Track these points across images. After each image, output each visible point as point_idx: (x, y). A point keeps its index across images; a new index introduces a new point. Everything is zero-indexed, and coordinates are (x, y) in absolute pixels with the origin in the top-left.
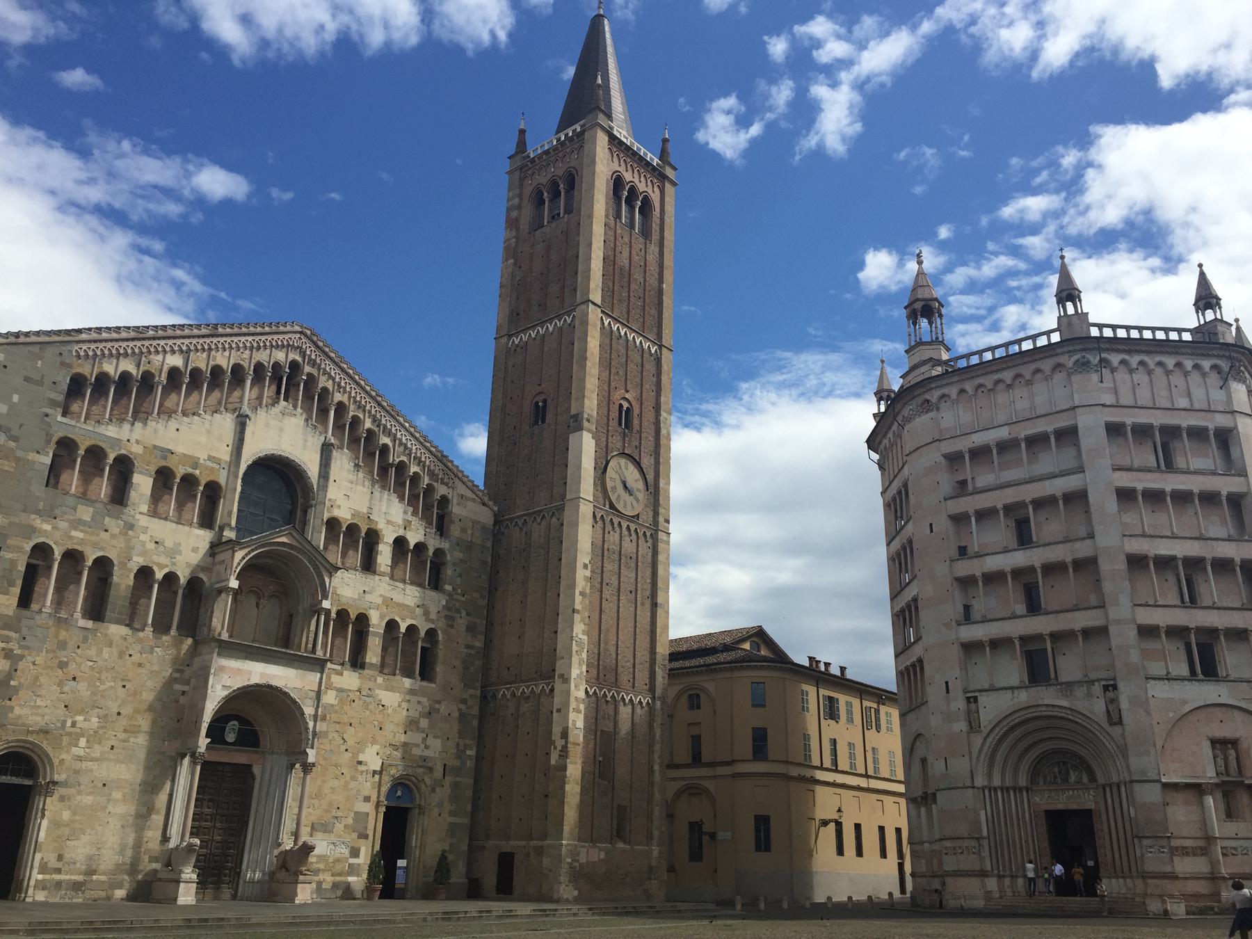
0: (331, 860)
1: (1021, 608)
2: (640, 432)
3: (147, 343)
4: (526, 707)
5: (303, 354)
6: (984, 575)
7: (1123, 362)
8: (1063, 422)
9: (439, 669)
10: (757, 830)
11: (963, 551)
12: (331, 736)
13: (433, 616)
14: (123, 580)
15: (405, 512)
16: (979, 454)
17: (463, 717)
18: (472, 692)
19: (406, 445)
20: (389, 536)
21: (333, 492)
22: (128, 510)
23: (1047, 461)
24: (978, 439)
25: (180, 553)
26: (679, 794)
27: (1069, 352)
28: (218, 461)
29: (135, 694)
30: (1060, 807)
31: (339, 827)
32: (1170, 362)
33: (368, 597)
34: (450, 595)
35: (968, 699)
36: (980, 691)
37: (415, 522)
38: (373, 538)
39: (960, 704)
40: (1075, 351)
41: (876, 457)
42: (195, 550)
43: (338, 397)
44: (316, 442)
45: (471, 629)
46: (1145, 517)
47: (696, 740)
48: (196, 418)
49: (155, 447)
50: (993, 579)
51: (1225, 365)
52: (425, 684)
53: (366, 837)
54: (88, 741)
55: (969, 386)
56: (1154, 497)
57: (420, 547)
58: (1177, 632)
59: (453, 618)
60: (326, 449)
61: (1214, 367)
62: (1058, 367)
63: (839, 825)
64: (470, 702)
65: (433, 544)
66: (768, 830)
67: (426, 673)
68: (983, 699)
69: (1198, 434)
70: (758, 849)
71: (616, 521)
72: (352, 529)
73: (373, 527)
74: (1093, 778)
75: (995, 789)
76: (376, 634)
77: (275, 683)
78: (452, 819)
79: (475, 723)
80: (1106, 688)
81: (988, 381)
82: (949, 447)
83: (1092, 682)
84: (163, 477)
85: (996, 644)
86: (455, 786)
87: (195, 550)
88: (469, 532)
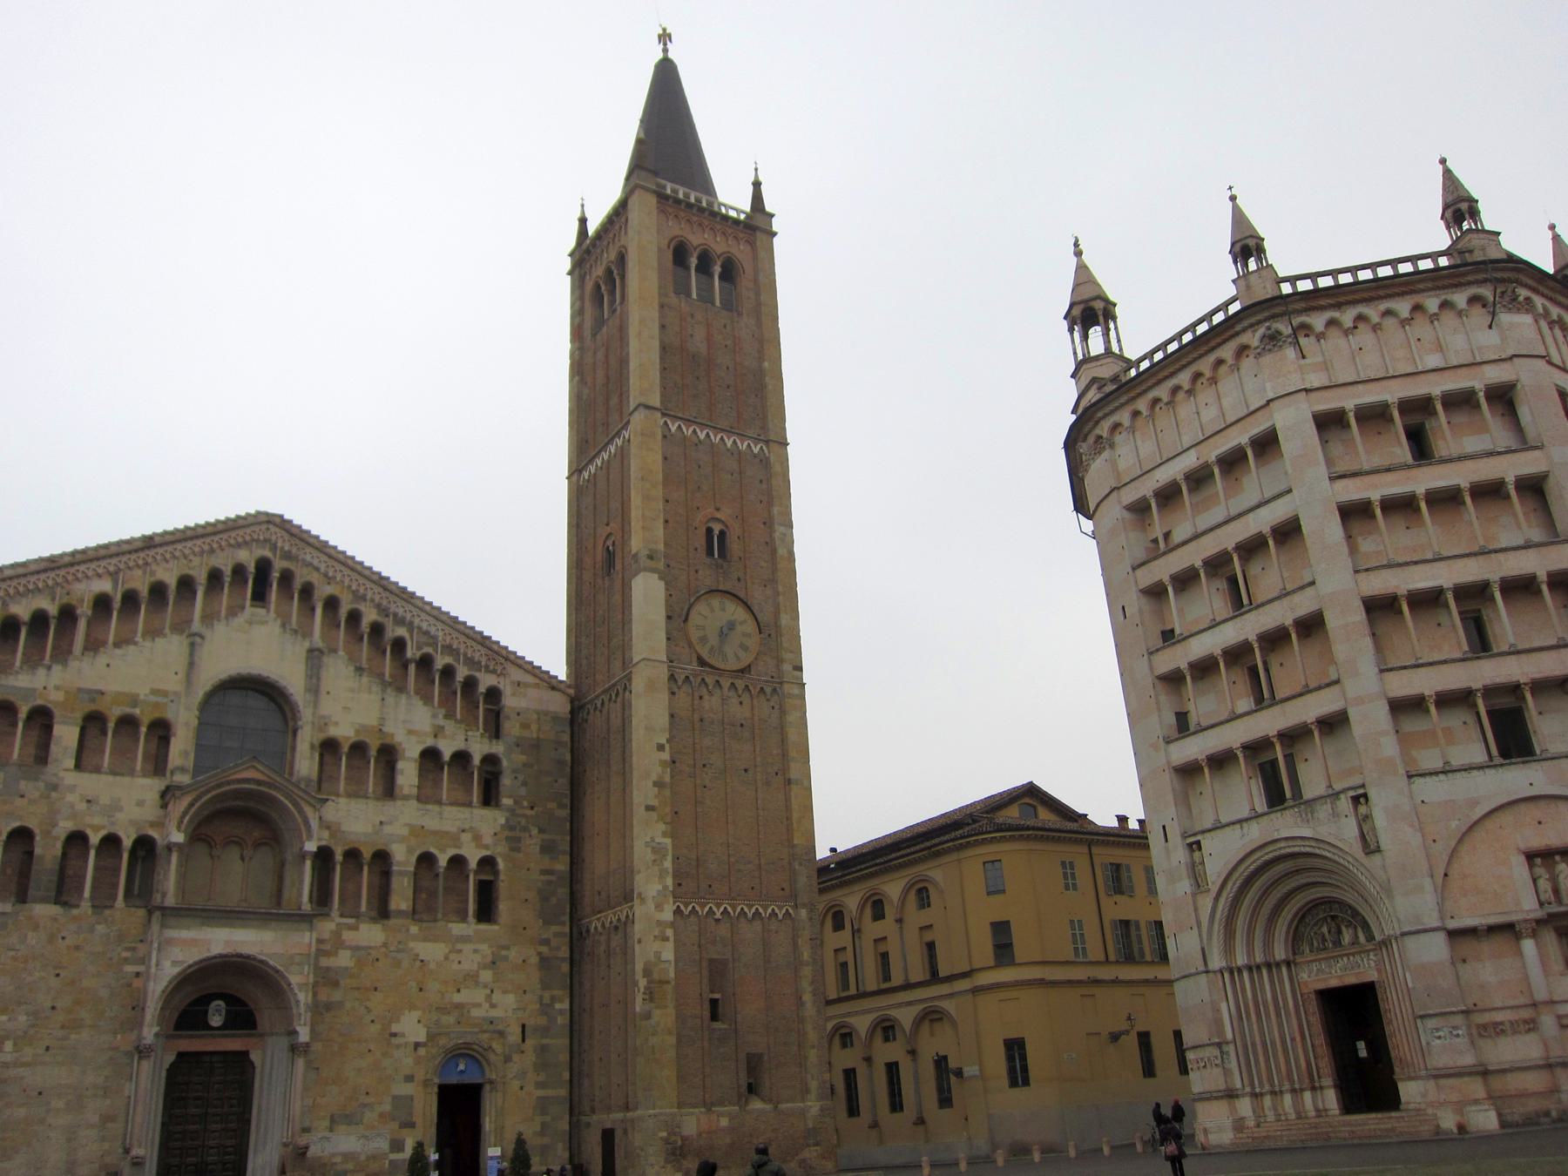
0: (363, 1157)
1: (1245, 704)
3: (62, 572)
4: (616, 940)
5: (274, 548)
6: (1192, 666)
7: (1332, 323)
8: (1257, 427)
9: (503, 907)
10: (1010, 1058)
11: (1168, 636)
12: (348, 1005)
13: (488, 840)
14: (48, 851)
15: (434, 716)
16: (1168, 496)
17: (544, 961)
18: (555, 928)
19: (427, 633)
20: (411, 750)
21: (328, 707)
22: (51, 768)
23: (1256, 481)
24: (1163, 476)
25: (121, 809)
26: (918, 1022)
27: (1252, 326)
28: (165, 693)
29: (73, 983)
30: (1334, 983)
31: (370, 1116)
32: (1403, 307)
33: (387, 829)
34: (512, 811)
35: (1190, 845)
36: (1203, 832)
37: (450, 726)
38: (389, 755)
39: (1180, 855)
40: (1259, 323)
41: (1088, 525)
42: (140, 803)
43: (329, 590)
44: (302, 647)
45: (548, 849)
46: (1388, 538)
47: (931, 946)
48: (132, 648)
49: (80, 690)
50: (1204, 669)
51: (1486, 292)
52: (483, 927)
53: (412, 1125)
54: (15, 1044)
55: (1142, 405)
56: (1401, 506)
57: (461, 757)
58: (1451, 700)
59: (519, 840)
60: (314, 657)
61: (1473, 300)
62: (1242, 350)
63: (1144, 1039)
64: (554, 943)
65: (479, 748)
66: (1023, 1058)
67: (486, 912)
68: (1206, 841)
69: (1460, 401)
70: (1013, 1084)
71: (710, 680)
72: (359, 748)
73: (388, 741)
74: (1370, 938)
75: (1240, 970)
76: (401, 873)
77: (245, 951)
78: (541, 1093)
79: (566, 967)
80: (1356, 800)
81: (1162, 392)
82: (1130, 495)
83: (1336, 795)
84: (93, 722)
85: (1221, 761)
86: (543, 1049)
87: (140, 803)
88: (534, 727)
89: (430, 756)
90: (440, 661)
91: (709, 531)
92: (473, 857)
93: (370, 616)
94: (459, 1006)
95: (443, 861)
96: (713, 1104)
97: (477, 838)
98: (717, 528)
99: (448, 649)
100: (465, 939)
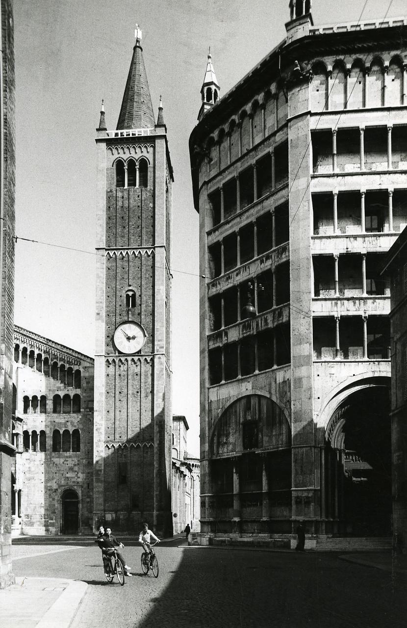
2: (140, 305)
13: (76, 424)
57: (67, 396)
65: (72, 392)
71: (123, 359)
89: (56, 398)
90: (60, 364)
91: (128, 296)
92: (71, 429)
93: (37, 352)
94: (67, 478)
95: (61, 432)
96: (118, 511)
97: (72, 423)
98: (130, 293)
99: (61, 360)
100: (70, 457)
